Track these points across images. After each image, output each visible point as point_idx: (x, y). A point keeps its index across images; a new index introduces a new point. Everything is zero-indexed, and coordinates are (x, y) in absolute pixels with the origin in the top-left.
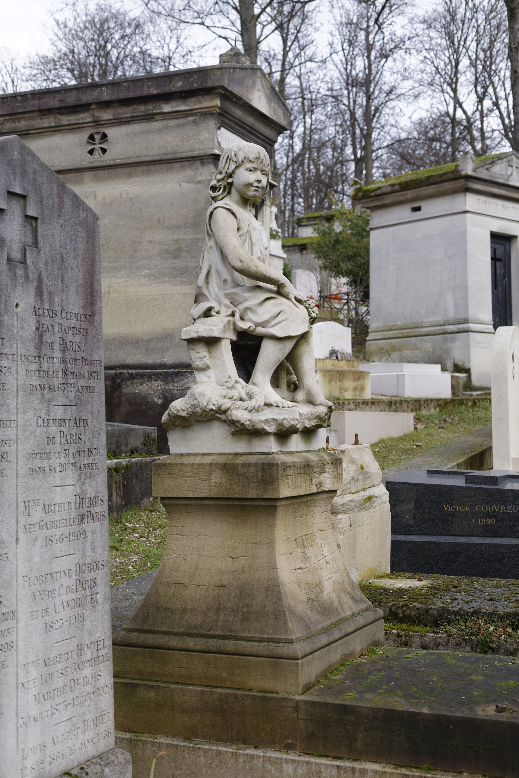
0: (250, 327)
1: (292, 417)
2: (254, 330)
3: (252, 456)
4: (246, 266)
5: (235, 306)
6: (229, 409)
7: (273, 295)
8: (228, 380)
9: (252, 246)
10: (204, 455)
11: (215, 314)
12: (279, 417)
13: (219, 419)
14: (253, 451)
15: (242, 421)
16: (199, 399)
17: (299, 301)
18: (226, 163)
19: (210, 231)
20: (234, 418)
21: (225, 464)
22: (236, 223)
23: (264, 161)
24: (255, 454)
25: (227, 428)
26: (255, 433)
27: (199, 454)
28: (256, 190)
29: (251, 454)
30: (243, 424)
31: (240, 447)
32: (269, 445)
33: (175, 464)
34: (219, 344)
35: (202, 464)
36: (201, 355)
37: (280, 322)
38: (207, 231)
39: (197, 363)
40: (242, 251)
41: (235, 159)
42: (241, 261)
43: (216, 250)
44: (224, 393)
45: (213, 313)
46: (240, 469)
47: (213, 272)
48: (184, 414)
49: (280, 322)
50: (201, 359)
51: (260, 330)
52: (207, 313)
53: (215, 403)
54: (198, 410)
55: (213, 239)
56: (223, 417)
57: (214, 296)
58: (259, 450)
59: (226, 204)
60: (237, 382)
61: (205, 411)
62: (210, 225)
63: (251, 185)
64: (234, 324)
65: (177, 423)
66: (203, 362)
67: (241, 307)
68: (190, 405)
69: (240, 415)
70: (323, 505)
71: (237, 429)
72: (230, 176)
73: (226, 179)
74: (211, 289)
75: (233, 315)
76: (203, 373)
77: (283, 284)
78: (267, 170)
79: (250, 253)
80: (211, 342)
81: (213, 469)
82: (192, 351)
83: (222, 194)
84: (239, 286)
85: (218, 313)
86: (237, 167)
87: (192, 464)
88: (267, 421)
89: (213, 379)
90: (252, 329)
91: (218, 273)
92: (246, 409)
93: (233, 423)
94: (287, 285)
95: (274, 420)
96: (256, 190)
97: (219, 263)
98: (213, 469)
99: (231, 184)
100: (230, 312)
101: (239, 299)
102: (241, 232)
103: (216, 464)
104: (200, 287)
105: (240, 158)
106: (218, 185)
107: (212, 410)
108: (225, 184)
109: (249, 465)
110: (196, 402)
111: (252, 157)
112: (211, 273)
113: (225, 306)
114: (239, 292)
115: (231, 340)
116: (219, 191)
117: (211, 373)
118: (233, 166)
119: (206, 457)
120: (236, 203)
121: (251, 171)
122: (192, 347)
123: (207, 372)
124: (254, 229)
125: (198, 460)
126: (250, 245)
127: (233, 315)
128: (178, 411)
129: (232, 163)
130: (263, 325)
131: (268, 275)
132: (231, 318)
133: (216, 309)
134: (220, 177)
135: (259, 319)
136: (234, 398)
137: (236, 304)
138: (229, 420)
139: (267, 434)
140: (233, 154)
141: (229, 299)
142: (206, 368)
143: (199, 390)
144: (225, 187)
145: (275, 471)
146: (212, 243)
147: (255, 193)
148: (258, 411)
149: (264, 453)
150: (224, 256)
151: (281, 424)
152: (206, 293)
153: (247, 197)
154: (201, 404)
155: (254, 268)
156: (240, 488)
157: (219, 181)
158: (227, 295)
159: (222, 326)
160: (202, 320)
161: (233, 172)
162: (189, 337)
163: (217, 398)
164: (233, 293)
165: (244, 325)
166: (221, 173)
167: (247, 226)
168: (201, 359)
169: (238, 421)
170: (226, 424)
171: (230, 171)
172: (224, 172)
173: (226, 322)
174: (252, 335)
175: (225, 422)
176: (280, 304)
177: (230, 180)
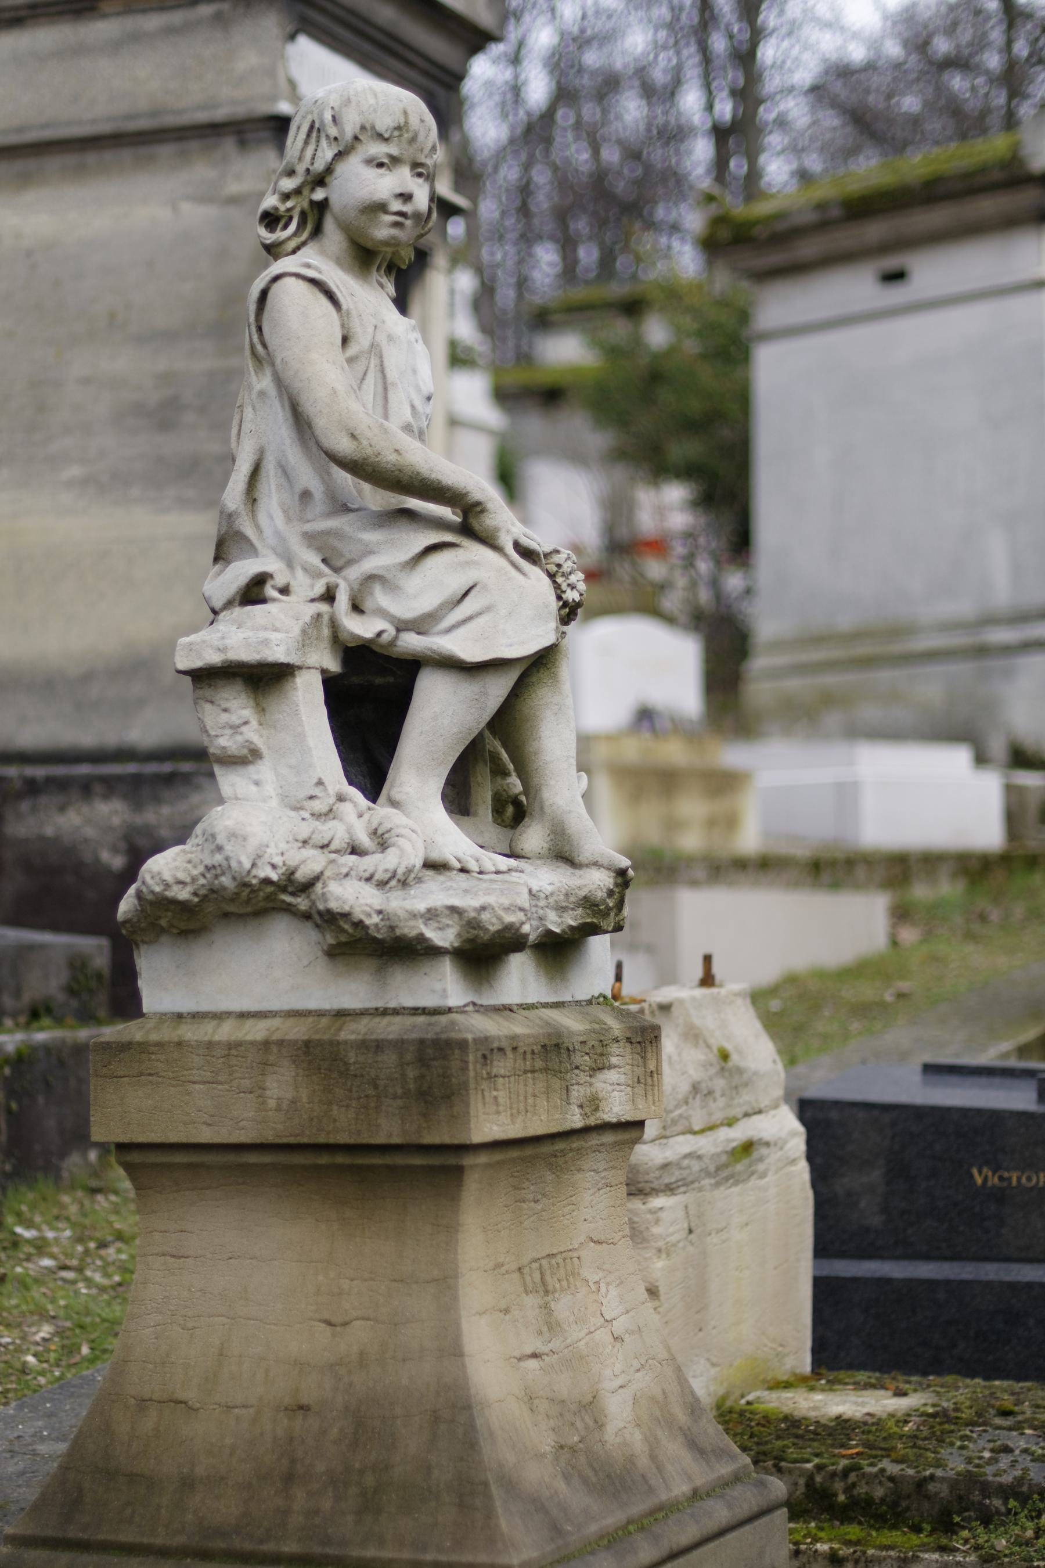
0: (380, 634)
1: (506, 902)
2: (393, 643)
3: (386, 1020)
4: (369, 451)
5: (337, 570)
6: (317, 878)
7: (449, 537)
8: (317, 791)
9: (385, 389)
10: (243, 1015)
11: (275, 594)
12: (469, 903)
13: (289, 909)
14: (392, 1005)
15: (358, 914)
16: (229, 848)
17: (528, 554)
18: (306, 142)
19: (259, 347)
20: (334, 905)
21: (307, 1044)
22: (337, 323)
23: (421, 137)
24: (396, 1012)
25: (313, 935)
26: (396, 950)
27: (227, 1015)
28: (397, 225)
29: (384, 1012)
30: (359, 924)
31: (352, 991)
32: (438, 986)
33: (160, 1044)
34: (288, 686)
35: (239, 1044)
36: (234, 719)
37: (470, 618)
38: (252, 347)
39: (223, 742)
40: (355, 406)
41: (333, 131)
42: (353, 436)
43: (277, 403)
44: (304, 830)
45: (270, 591)
46: (352, 1057)
47: (270, 468)
48: (183, 894)
49: (470, 618)
50: (235, 728)
51: (412, 642)
52: (253, 593)
53: (278, 860)
54: (226, 881)
55: (268, 372)
56: (302, 903)
57: (272, 541)
58: (409, 1002)
59: (308, 266)
60: (341, 798)
61: (246, 885)
62: (260, 329)
63: (381, 207)
64: (334, 625)
65: (163, 923)
66: (239, 738)
67: (354, 573)
68: (201, 869)
69: (352, 895)
70: (602, 1166)
71: (343, 938)
72: (320, 180)
73: (306, 192)
74: (262, 518)
75: (329, 596)
76: (242, 770)
77: (478, 504)
78: (429, 162)
79: (380, 410)
80: (264, 679)
81: (272, 1058)
82: (208, 707)
83: (296, 234)
84: (346, 509)
85: (285, 591)
86: (340, 155)
87: (210, 1045)
88: (431, 915)
89: (270, 789)
90: (386, 638)
91: (284, 471)
92: (368, 879)
93: (330, 920)
94: (490, 506)
95: (453, 910)
96: (397, 225)
97: (288, 441)
98: (272, 1058)
99: (322, 206)
100: (319, 588)
101: (348, 550)
102: (352, 351)
103: (281, 1043)
104: (230, 515)
105: (350, 128)
106: (282, 208)
107: (267, 881)
108: (305, 204)
109: (378, 1046)
110: (218, 858)
111: (384, 123)
112: (263, 473)
113: (305, 570)
114: (347, 529)
115: (323, 671)
116: (285, 227)
117: (263, 770)
118: (327, 153)
119: (250, 1023)
120: (339, 262)
121: (381, 165)
122: (208, 692)
123: (251, 768)
124: (390, 338)
125: (226, 1032)
126: (380, 389)
127: (329, 596)
128: (167, 886)
129: (324, 142)
130: (420, 625)
131: (433, 476)
132: (323, 607)
133: (280, 580)
134: (288, 184)
135: (408, 608)
136: (332, 847)
137: (339, 563)
138: (320, 913)
139: (433, 952)
140: (328, 116)
141: (319, 549)
142: (250, 757)
143: (229, 823)
144: (303, 215)
145: (455, 1064)
146: (264, 382)
147: (394, 232)
148: (404, 884)
149: (424, 1011)
150: (301, 422)
151: (473, 924)
152: (249, 531)
153: (369, 245)
154: (234, 864)
155: (392, 457)
156: (351, 1114)
157: (286, 197)
158: (312, 539)
159: (296, 631)
160: (238, 612)
161: (329, 170)
162: (198, 664)
163: (283, 846)
164: (328, 533)
165: (362, 628)
166: (291, 173)
167: (371, 330)
168: (235, 728)
169: (346, 916)
170: (309, 924)
171: (319, 166)
172: (301, 169)
173: (307, 619)
174: (388, 658)
175: (307, 916)
176: (469, 564)
177: (319, 195)
